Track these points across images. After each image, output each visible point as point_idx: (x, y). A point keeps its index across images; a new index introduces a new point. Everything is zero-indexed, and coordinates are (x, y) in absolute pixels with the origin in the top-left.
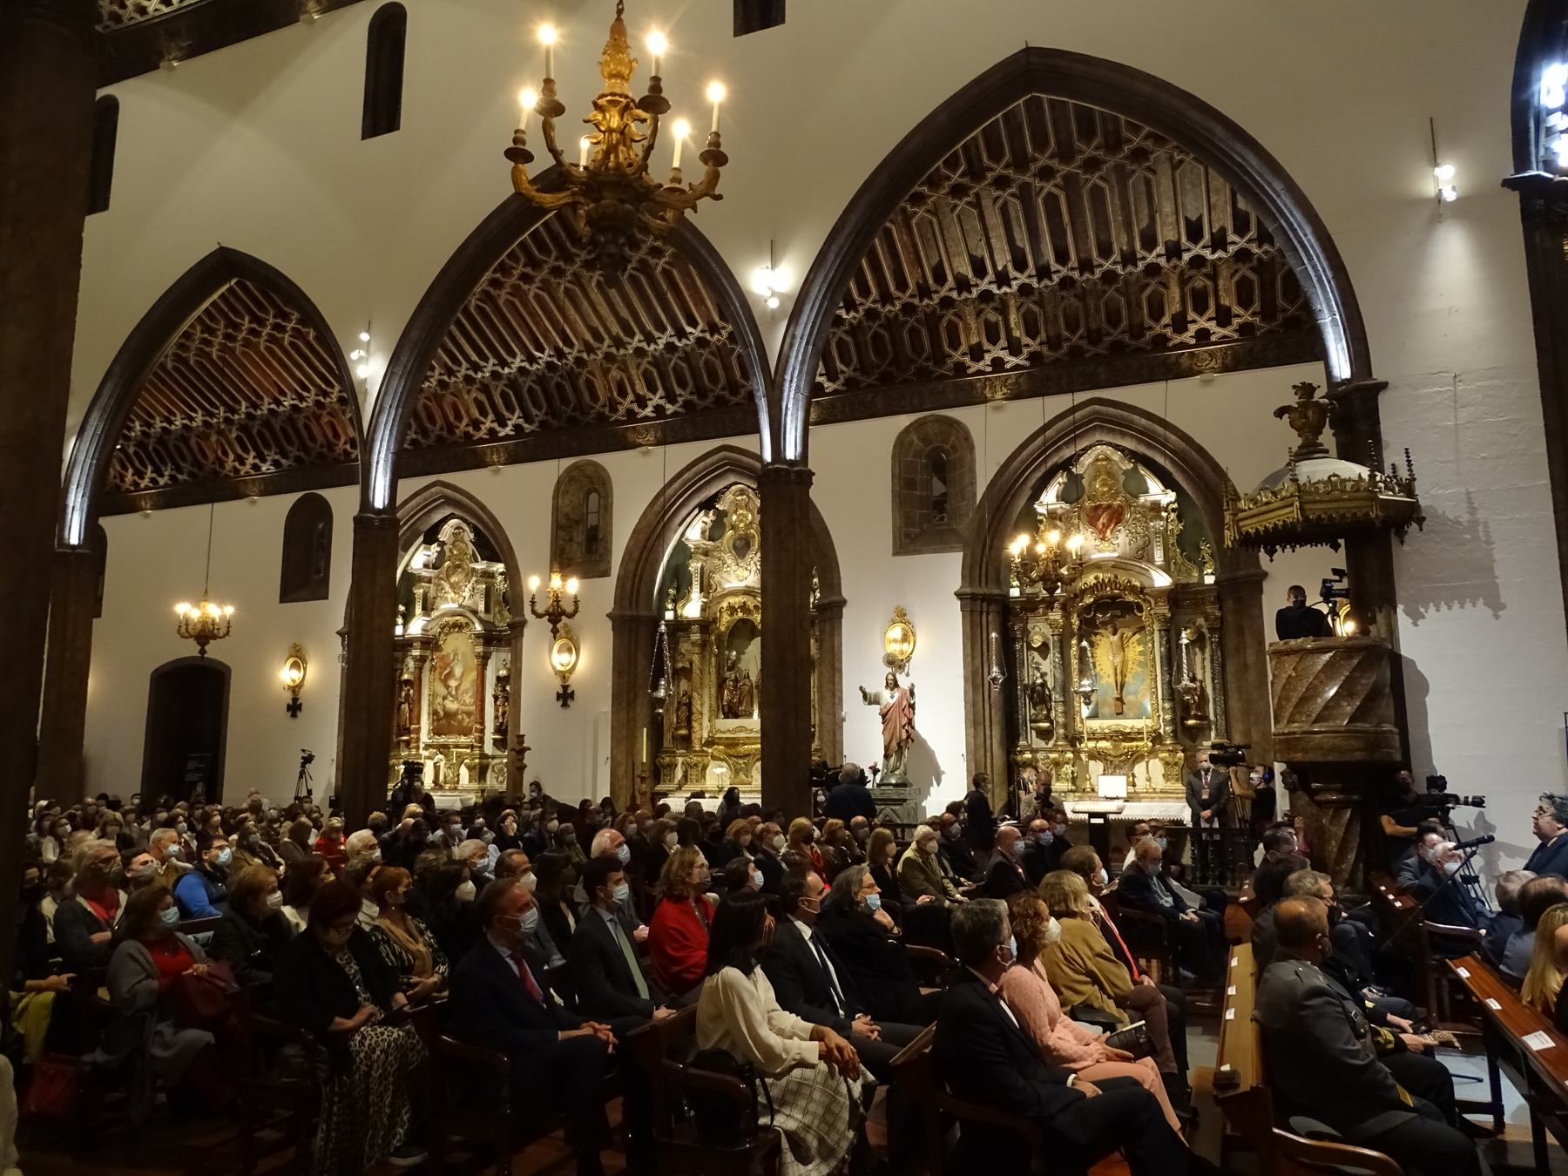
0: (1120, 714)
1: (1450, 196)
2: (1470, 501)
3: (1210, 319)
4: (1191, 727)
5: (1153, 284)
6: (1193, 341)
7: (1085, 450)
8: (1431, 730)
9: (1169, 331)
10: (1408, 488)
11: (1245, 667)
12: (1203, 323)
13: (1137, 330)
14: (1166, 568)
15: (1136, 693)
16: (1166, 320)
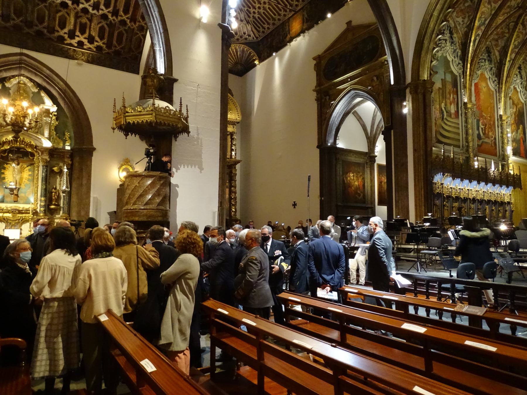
0: (16, 201)
1: (205, 20)
2: (198, 130)
3: (85, 38)
4: (52, 209)
5: (63, 12)
6: (76, 45)
7: (14, 77)
8: (177, 211)
9: (66, 36)
10: (186, 119)
11: (81, 185)
12: (82, 38)
13: (52, 30)
14: (49, 139)
15: (25, 193)
16: (66, 30)
